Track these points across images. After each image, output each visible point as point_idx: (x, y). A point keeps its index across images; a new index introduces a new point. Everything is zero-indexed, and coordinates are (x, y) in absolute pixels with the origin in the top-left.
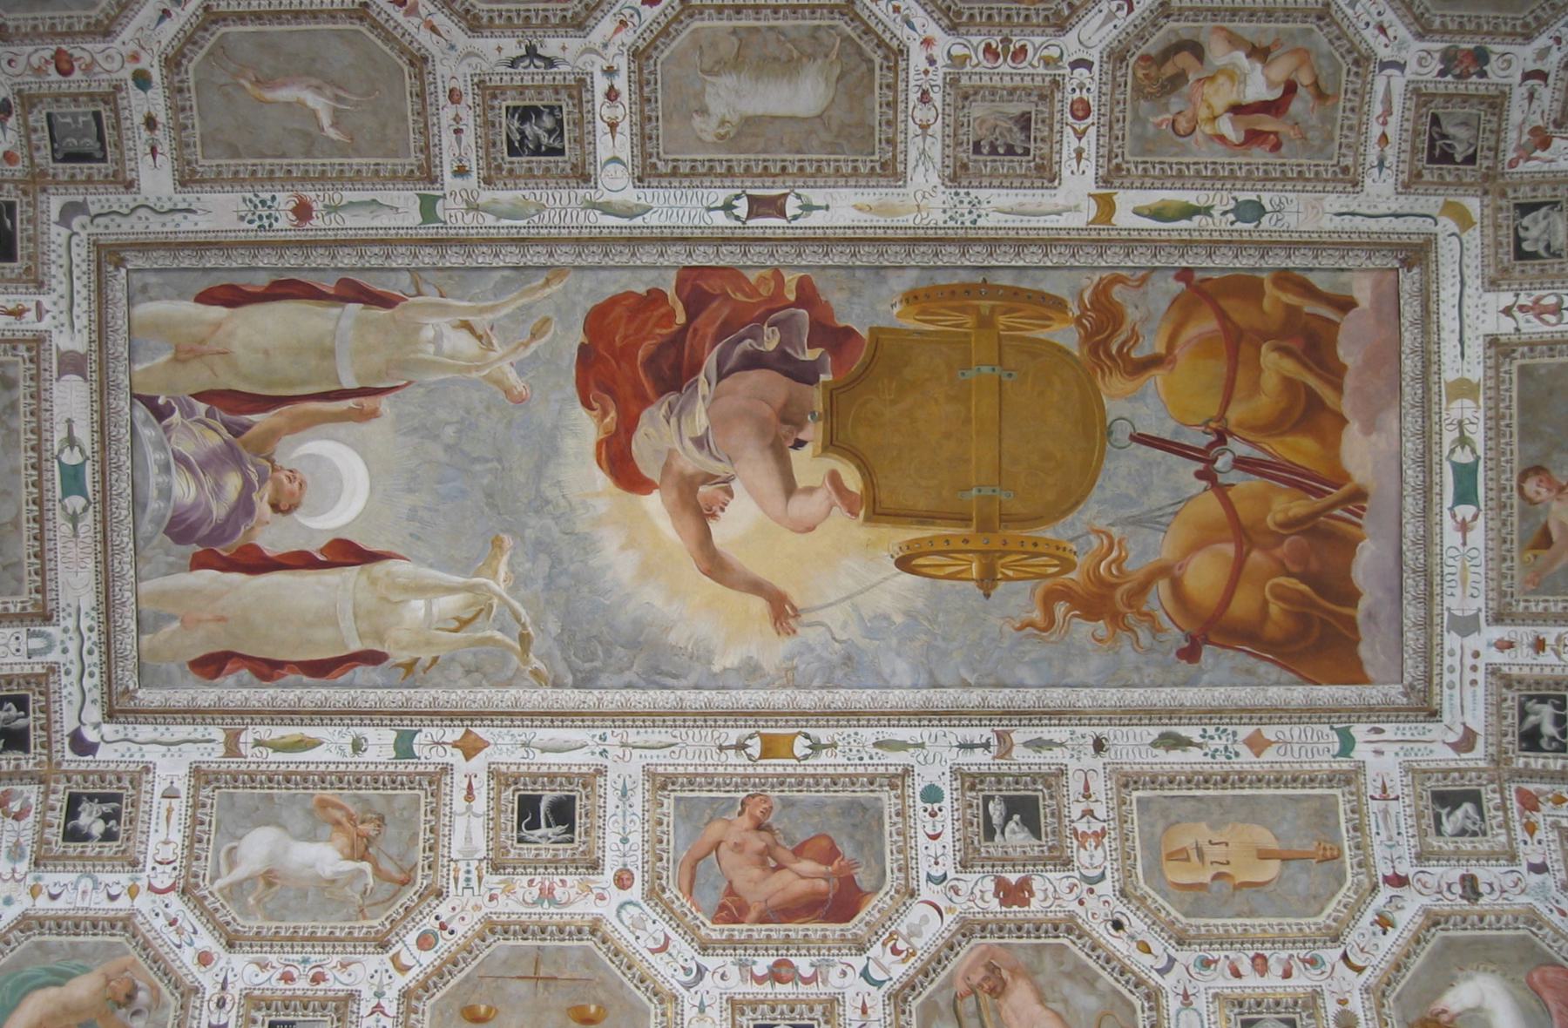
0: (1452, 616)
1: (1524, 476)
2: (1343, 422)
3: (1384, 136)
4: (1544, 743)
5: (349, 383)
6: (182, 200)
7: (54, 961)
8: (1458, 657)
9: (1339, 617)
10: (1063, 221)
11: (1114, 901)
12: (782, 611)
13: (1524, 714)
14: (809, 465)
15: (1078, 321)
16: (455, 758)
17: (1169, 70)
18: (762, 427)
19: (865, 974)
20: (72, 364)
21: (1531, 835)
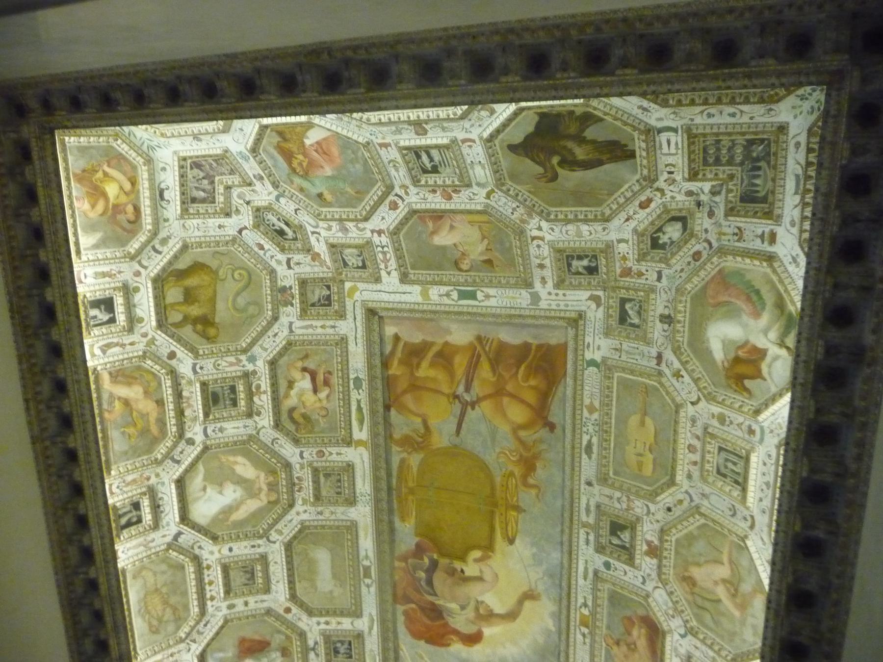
0: (531, 304)
1: (460, 270)
2: (446, 344)
3: (322, 327)
4: (594, 265)
8: (552, 302)
9: (537, 351)
11: (658, 506)
12: (530, 596)
14: (471, 569)
15: (409, 453)
17: (301, 420)
21: (643, 274)
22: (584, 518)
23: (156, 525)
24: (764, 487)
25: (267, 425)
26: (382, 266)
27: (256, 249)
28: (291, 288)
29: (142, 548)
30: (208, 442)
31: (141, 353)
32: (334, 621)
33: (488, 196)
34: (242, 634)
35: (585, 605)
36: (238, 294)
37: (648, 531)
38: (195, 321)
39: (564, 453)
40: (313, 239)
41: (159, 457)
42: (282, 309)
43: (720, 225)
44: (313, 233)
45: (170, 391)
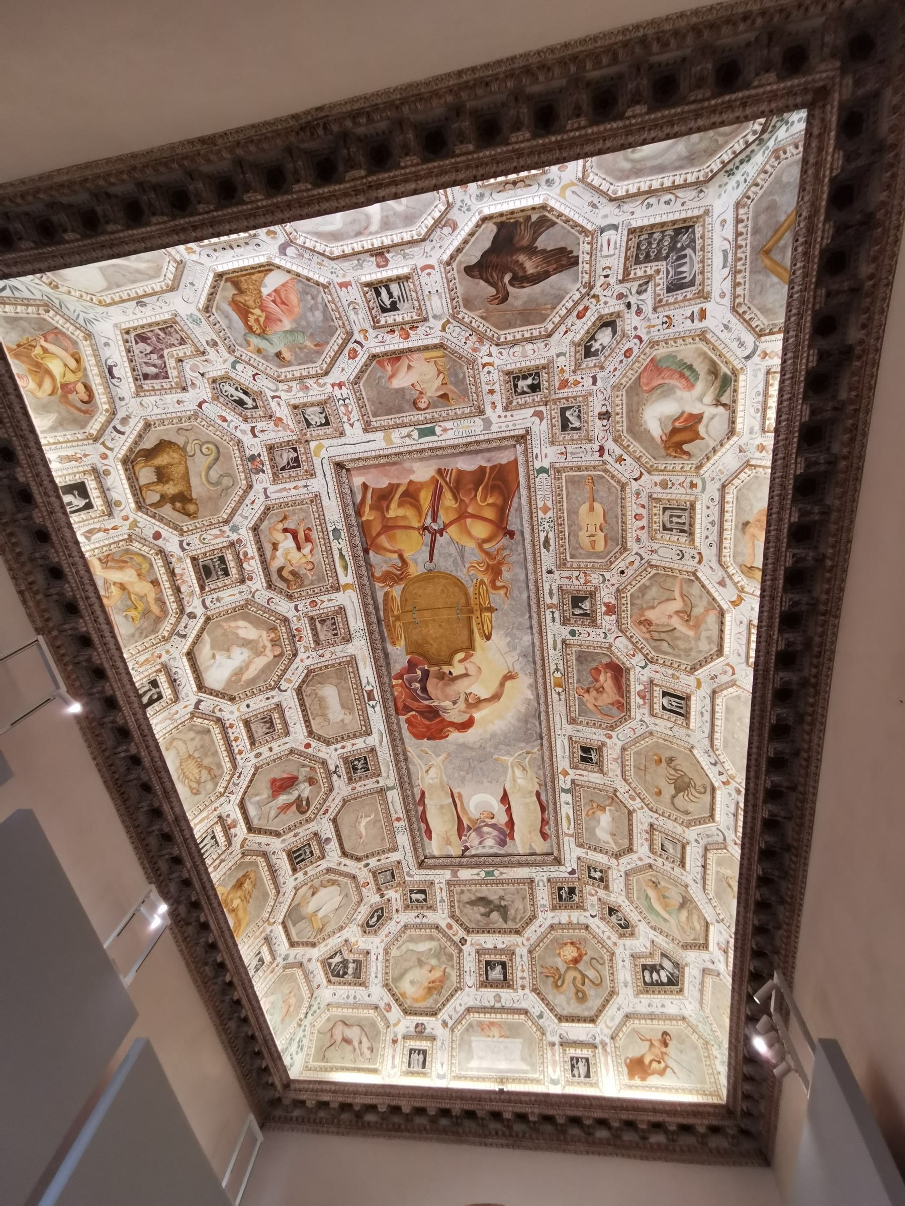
1: (419, 409)
2: (411, 482)
4: (536, 382)
5: (451, 800)
6: (401, 849)
7: (643, 898)
9: (490, 474)
10: (355, 601)
13: (524, 393)
14: (457, 669)
16: (569, 778)
17: (290, 577)
18: (446, 685)
19: (643, 668)
20: (454, 874)
22: (548, 601)
23: (176, 699)
24: (709, 526)
25: (260, 588)
26: (345, 419)
27: (219, 422)
28: (259, 455)
29: (168, 721)
30: (209, 613)
31: (126, 536)
32: (348, 744)
33: (443, 329)
34: (272, 776)
35: (557, 670)
36: (210, 468)
37: (606, 595)
38: (173, 499)
39: (525, 553)
40: (273, 404)
41: (166, 634)
42: (254, 477)
43: (649, 319)
44: (273, 397)
45: (163, 570)
